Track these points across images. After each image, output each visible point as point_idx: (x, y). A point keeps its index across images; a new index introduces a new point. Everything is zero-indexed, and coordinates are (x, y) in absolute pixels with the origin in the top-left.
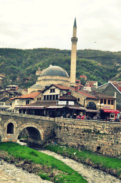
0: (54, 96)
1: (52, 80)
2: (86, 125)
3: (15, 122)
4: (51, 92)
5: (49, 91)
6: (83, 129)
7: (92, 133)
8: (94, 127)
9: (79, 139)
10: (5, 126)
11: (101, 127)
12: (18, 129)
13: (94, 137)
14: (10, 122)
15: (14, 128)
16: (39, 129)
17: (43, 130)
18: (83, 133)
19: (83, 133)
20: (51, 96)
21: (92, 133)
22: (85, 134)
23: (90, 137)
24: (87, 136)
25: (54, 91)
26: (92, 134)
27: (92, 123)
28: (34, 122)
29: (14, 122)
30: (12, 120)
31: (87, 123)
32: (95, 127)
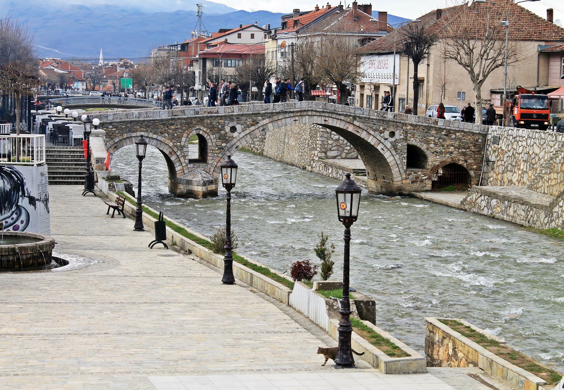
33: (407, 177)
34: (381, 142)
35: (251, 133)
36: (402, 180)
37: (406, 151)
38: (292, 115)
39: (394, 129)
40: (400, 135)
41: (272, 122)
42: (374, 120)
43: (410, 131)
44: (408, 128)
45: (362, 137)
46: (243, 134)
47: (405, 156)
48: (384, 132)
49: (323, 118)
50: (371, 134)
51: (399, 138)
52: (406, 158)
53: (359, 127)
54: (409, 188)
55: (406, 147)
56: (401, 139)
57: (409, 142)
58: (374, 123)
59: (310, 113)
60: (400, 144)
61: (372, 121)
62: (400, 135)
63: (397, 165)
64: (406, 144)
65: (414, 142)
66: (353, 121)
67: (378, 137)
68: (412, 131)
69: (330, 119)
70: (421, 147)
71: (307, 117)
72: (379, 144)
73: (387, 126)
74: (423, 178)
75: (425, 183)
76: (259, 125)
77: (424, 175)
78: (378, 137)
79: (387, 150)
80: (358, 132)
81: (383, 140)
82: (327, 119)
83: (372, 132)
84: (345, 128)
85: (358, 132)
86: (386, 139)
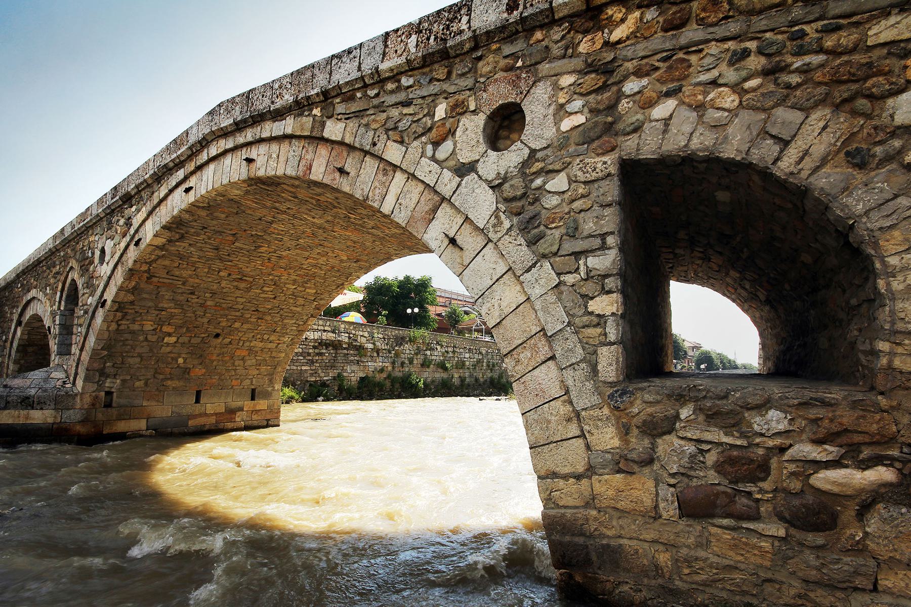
2: (325, 331)
6: (315, 340)
7: (345, 349)
8: (347, 335)
9: (304, 368)
11: (366, 334)
13: (352, 358)
18: (317, 351)
19: (317, 351)
21: (345, 349)
22: (324, 351)
23: (339, 358)
24: (329, 358)
26: (345, 351)
27: (343, 326)
31: (328, 324)
32: (351, 335)
33: (639, 444)
34: (443, 199)
35: (124, 259)
36: (590, 471)
37: (610, 220)
38: (180, 174)
39: (515, 84)
40: (561, 111)
41: (150, 214)
42: (405, 81)
43: (641, 49)
44: (619, 33)
45: (358, 195)
46: (111, 265)
47: (602, 262)
48: (452, 133)
49: (244, 153)
50: (395, 167)
51: (550, 133)
52: (610, 283)
53: (341, 143)
54: (664, 558)
55: (611, 190)
56: (564, 139)
57: (629, 146)
58: (401, 96)
59: (213, 151)
60: (559, 183)
61: (399, 89)
62: (561, 111)
63: (550, 339)
64: (607, 163)
65: (685, 121)
66: (323, 125)
67: (427, 170)
68: (659, 41)
69: (263, 148)
70: (765, 152)
71: (212, 166)
72: (435, 210)
73: (469, 82)
74: (825, 479)
75: (859, 549)
76: (132, 231)
77: (830, 452)
78: (427, 170)
79: (480, 241)
80: (342, 171)
81: (447, 182)
82: (253, 153)
83: (393, 153)
84: (301, 173)
85: (342, 171)
86: (464, 170)
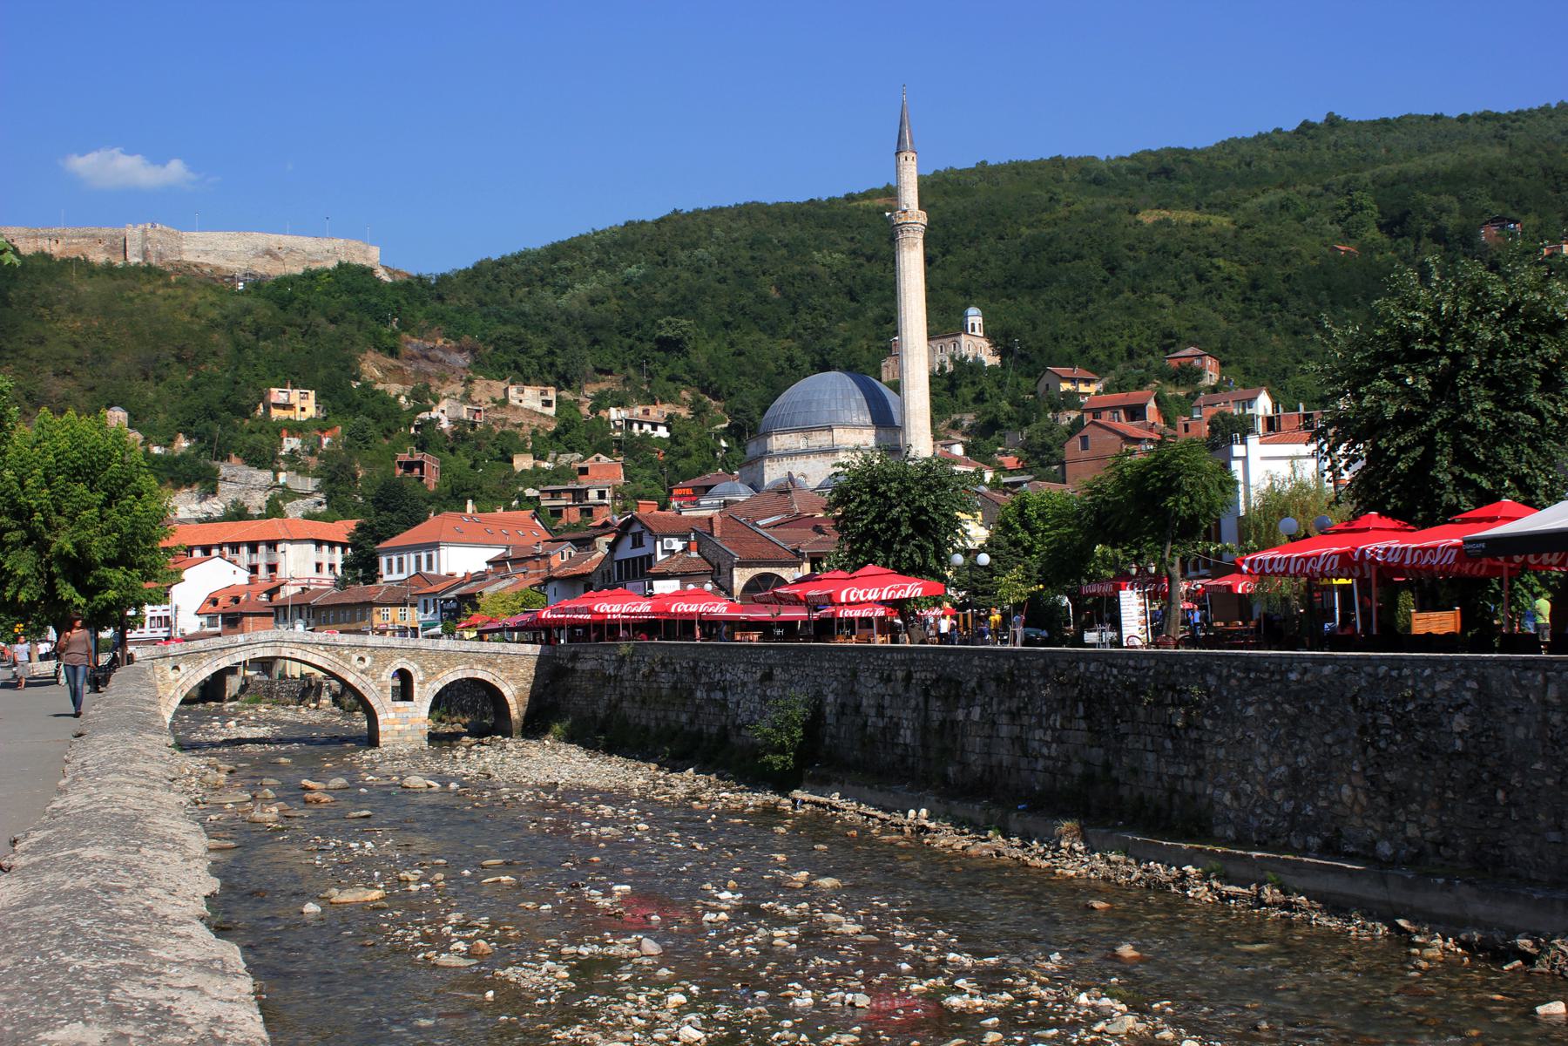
0: (641, 558)
1: (807, 453)
3: (416, 666)
4: (634, 546)
5: (628, 541)
10: (383, 678)
12: (428, 686)
14: (399, 666)
15: (415, 684)
16: (498, 684)
17: (513, 688)
20: (634, 559)
25: (641, 545)
28: (479, 661)
29: (411, 667)
30: (404, 659)
